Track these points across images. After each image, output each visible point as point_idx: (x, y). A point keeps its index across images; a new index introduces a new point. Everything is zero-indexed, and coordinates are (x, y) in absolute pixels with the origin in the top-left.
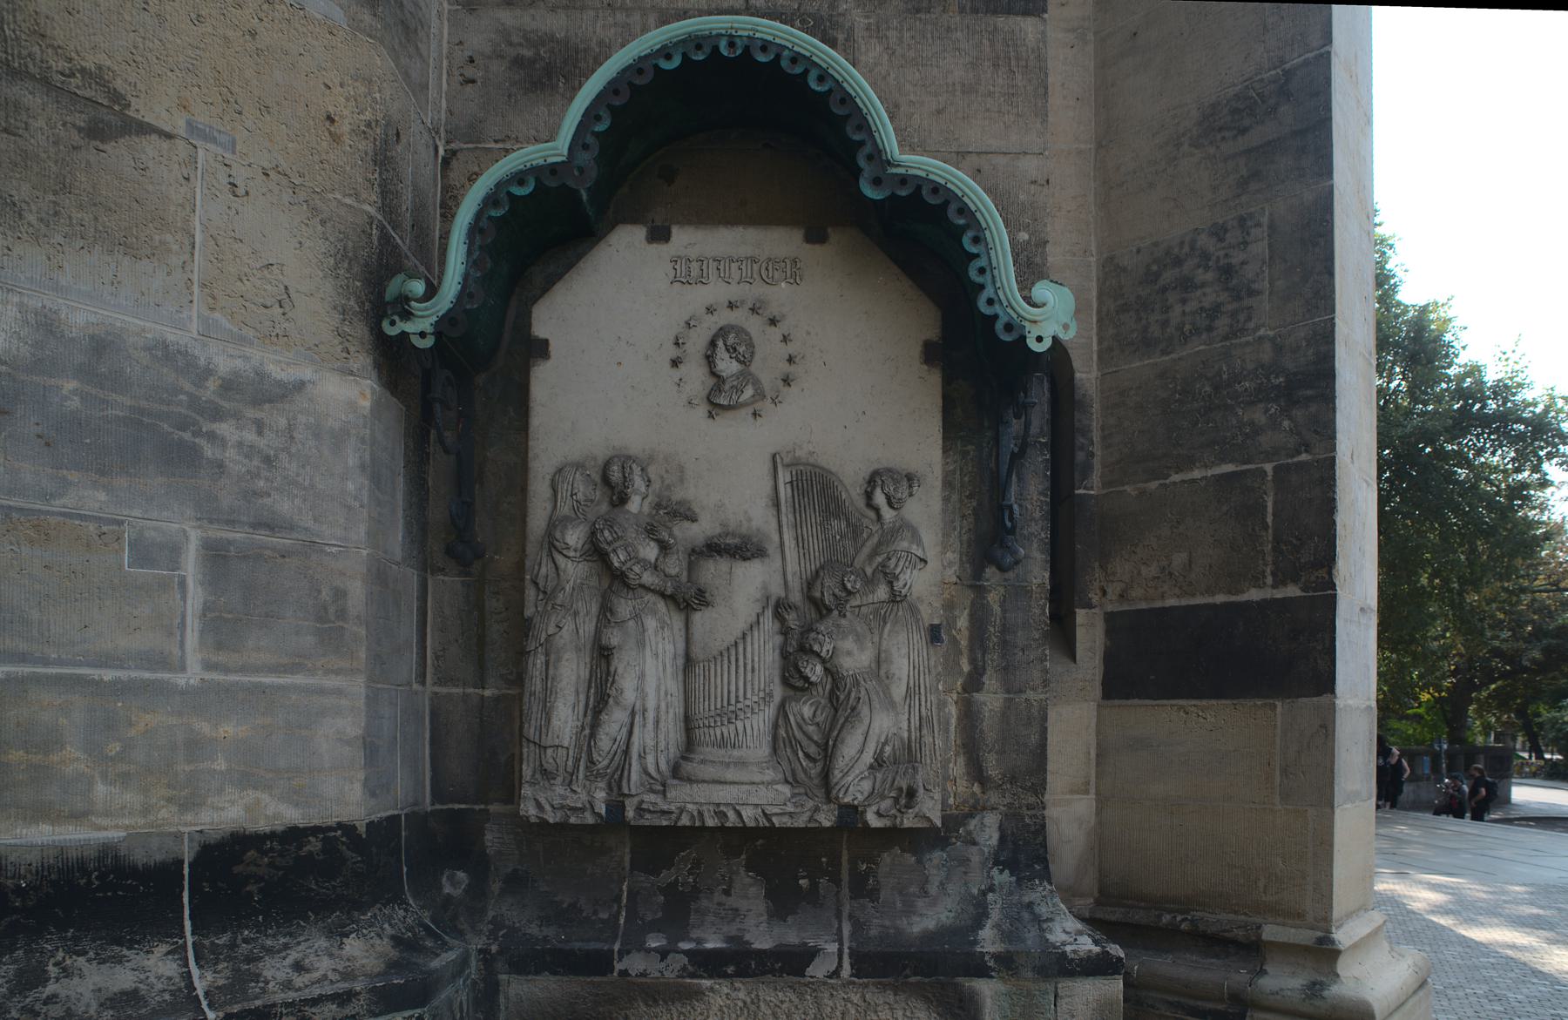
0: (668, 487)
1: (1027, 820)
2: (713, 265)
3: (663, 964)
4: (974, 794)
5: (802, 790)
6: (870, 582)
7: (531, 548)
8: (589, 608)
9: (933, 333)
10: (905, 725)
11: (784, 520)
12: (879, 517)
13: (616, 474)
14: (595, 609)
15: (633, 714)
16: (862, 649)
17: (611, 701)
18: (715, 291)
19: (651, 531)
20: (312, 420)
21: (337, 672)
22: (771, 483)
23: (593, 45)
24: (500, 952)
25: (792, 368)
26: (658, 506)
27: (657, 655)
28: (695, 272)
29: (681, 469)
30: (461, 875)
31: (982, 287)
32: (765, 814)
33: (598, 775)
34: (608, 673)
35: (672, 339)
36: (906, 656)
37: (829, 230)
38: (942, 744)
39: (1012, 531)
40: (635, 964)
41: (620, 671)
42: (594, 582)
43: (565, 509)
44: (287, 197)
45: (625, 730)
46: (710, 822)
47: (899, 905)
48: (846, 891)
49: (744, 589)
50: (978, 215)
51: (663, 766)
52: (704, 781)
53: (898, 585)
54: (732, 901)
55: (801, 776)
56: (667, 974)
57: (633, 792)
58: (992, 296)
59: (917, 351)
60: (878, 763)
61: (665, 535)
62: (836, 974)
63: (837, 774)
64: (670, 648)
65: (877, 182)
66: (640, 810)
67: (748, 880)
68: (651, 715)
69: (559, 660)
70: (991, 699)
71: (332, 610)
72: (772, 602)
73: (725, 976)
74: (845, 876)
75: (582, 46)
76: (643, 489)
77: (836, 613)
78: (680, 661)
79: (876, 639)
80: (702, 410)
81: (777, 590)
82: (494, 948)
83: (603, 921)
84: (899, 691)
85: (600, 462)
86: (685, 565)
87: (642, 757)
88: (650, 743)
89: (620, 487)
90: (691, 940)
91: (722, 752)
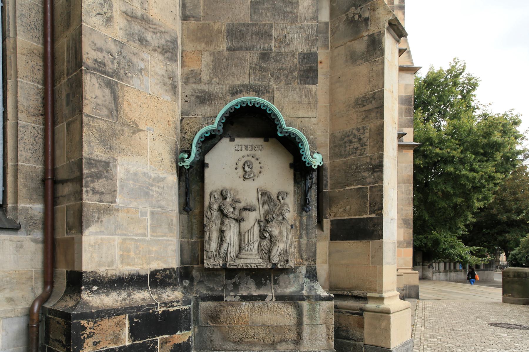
6: (278, 216)
7: (205, 209)
8: (219, 222)
13: (224, 193)
14: (220, 222)
18: (244, 153)
19: (232, 205)
21: (172, 236)
25: (261, 170)
26: (233, 200)
28: (240, 148)
29: (238, 192)
31: (303, 155)
36: (286, 231)
38: (293, 250)
39: (309, 204)
40: (228, 298)
42: (219, 216)
43: (213, 201)
46: (245, 267)
48: (272, 283)
49: (252, 218)
53: (284, 216)
54: (248, 286)
55: (264, 257)
59: (288, 166)
60: (280, 254)
61: (235, 206)
62: (271, 300)
63: (272, 257)
65: (281, 133)
66: (230, 265)
68: (232, 245)
70: (304, 241)
74: (272, 280)
78: (238, 233)
80: (242, 179)
81: (258, 218)
85: (220, 190)
88: (232, 251)
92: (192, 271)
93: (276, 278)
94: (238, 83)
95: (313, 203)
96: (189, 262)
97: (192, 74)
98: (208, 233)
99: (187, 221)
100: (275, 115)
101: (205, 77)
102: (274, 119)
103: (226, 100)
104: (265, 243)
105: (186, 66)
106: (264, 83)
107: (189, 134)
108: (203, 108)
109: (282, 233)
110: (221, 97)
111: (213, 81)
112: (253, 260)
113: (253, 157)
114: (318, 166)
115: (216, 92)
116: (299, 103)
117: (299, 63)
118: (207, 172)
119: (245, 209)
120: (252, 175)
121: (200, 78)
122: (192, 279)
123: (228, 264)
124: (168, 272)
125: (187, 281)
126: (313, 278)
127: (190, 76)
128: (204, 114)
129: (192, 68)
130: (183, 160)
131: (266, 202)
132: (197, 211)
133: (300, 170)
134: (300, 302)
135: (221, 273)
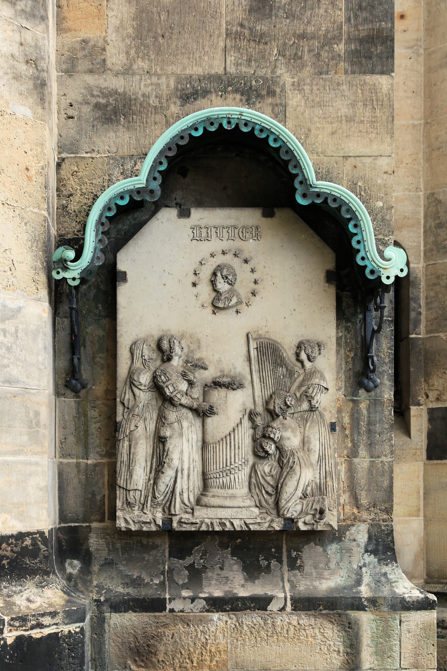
0: (192, 351)
1: (383, 528)
2: (213, 230)
3: (192, 605)
5: (264, 511)
6: (299, 400)
7: (120, 384)
9: (331, 266)
12: (303, 366)
13: (165, 345)
14: (155, 416)
15: (177, 471)
17: (166, 465)
18: (215, 245)
19: (184, 375)
20: (24, 326)
21: (36, 454)
22: (245, 349)
23: (139, 96)
24: (106, 601)
25: (256, 287)
26: (187, 362)
27: (188, 440)
28: (204, 235)
29: (199, 341)
30: (76, 562)
31: (358, 251)
34: (164, 450)
35: (193, 271)
38: (337, 486)
39: (373, 371)
40: (177, 605)
42: (154, 402)
44: (11, 214)
45: (172, 480)
46: (217, 528)
50: (357, 213)
51: (192, 499)
52: (214, 507)
53: (314, 402)
55: (264, 503)
57: (177, 513)
58: (364, 256)
59: (322, 276)
60: (305, 496)
61: (191, 377)
62: (283, 609)
64: (195, 436)
65: (304, 196)
66: (180, 522)
67: (232, 562)
68: (186, 472)
69: (136, 444)
70: (363, 461)
71: (34, 422)
72: (248, 411)
73: (225, 611)
75: (133, 97)
76: (180, 353)
77: (281, 417)
78: (200, 444)
79: (302, 430)
80: (210, 309)
82: (102, 599)
83: (156, 584)
85: (156, 338)
86: (201, 392)
87: (181, 494)
88: (185, 487)
89: (168, 352)
90: (205, 593)
91: (223, 491)
93: (294, 554)
94: (197, 71)
95: (385, 368)
97: (84, 49)
98: (126, 444)
99: (74, 412)
100: (289, 151)
101: (115, 57)
102: (286, 163)
103: (168, 113)
104: (267, 468)
105: (69, 30)
106: (261, 72)
107: (77, 198)
108: (112, 134)
109: (309, 442)
110: (155, 108)
111: (135, 67)
113: (235, 255)
114: (397, 277)
115: (144, 95)
116: (349, 120)
117: (349, 20)
118: (124, 293)
119: (217, 384)
120: (234, 300)
121: (104, 60)
124: (28, 542)
126: (384, 553)
127: (80, 55)
129: (83, 35)
130: (63, 264)
131: (268, 366)
132: (99, 389)
134: (353, 614)
135: (158, 541)
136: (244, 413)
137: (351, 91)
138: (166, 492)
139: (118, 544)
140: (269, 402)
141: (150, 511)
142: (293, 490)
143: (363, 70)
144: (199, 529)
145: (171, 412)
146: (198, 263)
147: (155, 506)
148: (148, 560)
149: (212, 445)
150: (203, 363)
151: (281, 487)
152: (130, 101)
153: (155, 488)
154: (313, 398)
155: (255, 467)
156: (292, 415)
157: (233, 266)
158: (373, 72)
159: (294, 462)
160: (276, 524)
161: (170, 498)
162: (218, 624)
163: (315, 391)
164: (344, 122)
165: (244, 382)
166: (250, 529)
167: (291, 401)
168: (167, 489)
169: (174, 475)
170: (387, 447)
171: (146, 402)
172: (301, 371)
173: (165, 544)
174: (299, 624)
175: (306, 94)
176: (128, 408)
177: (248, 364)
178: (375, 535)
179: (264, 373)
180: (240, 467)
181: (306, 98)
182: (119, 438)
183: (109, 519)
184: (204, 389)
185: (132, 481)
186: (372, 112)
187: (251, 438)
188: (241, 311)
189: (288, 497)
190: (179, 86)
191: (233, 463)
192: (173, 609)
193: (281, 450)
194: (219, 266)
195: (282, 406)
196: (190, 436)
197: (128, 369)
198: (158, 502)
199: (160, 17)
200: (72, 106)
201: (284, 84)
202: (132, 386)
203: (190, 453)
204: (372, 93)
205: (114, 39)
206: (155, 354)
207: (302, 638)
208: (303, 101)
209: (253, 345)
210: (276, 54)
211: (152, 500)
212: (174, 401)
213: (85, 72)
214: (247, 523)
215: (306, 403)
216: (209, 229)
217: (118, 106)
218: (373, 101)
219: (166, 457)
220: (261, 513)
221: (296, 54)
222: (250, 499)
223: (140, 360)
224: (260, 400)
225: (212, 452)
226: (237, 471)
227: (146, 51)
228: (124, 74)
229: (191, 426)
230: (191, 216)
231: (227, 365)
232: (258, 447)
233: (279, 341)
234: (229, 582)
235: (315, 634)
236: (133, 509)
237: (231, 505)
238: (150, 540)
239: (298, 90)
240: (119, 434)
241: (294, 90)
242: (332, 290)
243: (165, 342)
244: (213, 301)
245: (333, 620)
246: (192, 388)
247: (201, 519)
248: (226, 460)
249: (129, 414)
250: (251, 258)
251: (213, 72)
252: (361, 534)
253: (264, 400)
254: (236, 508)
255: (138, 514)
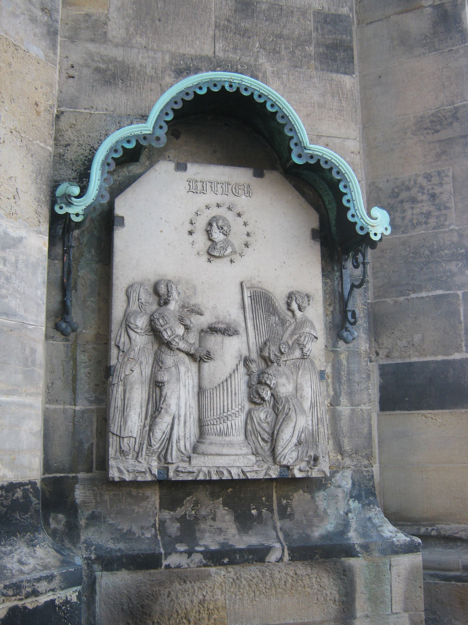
2: (209, 185)
3: (189, 560)
4: (338, 460)
7: (115, 327)
9: (316, 225)
10: (310, 423)
11: (247, 315)
12: (294, 315)
13: (162, 289)
16: (289, 383)
17: (163, 411)
18: (210, 198)
19: (181, 320)
22: (239, 297)
23: (137, 66)
26: (183, 307)
27: (185, 386)
28: (200, 187)
29: (194, 288)
32: (243, 472)
33: (154, 452)
34: (161, 395)
35: (189, 221)
37: (265, 171)
40: (173, 560)
41: (169, 395)
42: (150, 346)
43: (134, 307)
45: (169, 427)
46: (215, 477)
47: (305, 522)
48: (276, 516)
51: (188, 447)
52: (211, 455)
53: (305, 350)
54: (218, 524)
55: (260, 451)
56: (191, 565)
57: (174, 461)
59: (308, 233)
60: (299, 443)
61: (188, 322)
62: (280, 560)
63: (279, 449)
64: (191, 382)
66: (177, 471)
67: (224, 512)
68: (182, 419)
69: (132, 389)
73: (223, 564)
75: (131, 66)
76: (177, 298)
77: (275, 364)
78: (196, 390)
79: (295, 378)
80: (206, 257)
82: (93, 557)
83: (148, 539)
84: (307, 405)
87: (178, 441)
88: (182, 434)
89: (166, 297)
90: (200, 546)
91: (220, 438)
92: (73, 490)
94: (190, 51)
96: (67, 466)
97: (87, 21)
98: (121, 388)
101: (115, 30)
103: (163, 83)
104: (263, 414)
106: (246, 59)
107: (74, 148)
108: (110, 95)
110: (152, 77)
111: (134, 41)
112: (234, 458)
113: (229, 208)
115: (141, 65)
116: (321, 106)
117: (317, 29)
118: (121, 238)
119: (213, 330)
121: (105, 33)
122: (72, 510)
123: (172, 468)
124: (19, 494)
125: (61, 516)
128: (112, 108)
129: (86, 10)
133: (338, 240)
135: (148, 492)
136: (240, 359)
137: (321, 84)
138: (162, 439)
139: (106, 496)
140: (264, 349)
141: (145, 459)
142: (288, 437)
143: (330, 69)
144: (196, 478)
145: (168, 356)
146: (194, 213)
147: (150, 454)
148: (138, 512)
149: (209, 391)
150: (199, 309)
151: (277, 434)
152: (128, 68)
153: (151, 435)
154: (305, 346)
155: (251, 413)
156: (285, 362)
157: (227, 218)
158: (338, 72)
159: (290, 409)
160: (272, 472)
161: (166, 445)
162: (216, 579)
163: (307, 339)
164: (316, 107)
165: (239, 329)
166: (247, 477)
167: (285, 348)
168: (164, 436)
169: (171, 421)
170: (365, 396)
171: (142, 346)
172: (292, 321)
173: (156, 495)
174: (296, 574)
175: (284, 82)
176: (123, 352)
177: (243, 312)
178: (358, 481)
179: (258, 321)
180: (237, 413)
181: (284, 85)
182: (113, 383)
183: (97, 469)
184: (200, 334)
185: (127, 428)
186: (339, 102)
187: (246, 384)
188: (235, 261)
189: (285, 444)
190: (174, 62)
191: (230, 410)
192: (169, 565)
193: (276, 397)
194: (214, 217)
195: (277, 353)
196: (187, 381)
197: (124, 312)
198: (154, 450)
199: (157, 5)
200: (73, 67)
201: (265, 72)
202: (128, 328)
203: (186, 399)
204: (338, 88)
205: (115, 17)
206: (151, 298)
207: (299, 588)
208: (282, 87)
209: (247, 294)
210: (258, 47)
211: (147, 448)
212: (172, 345)
213: (87, 41)
214: (245, 471)
215: (298, 350)
216: (205, 183)
217: (117, 72)
218: (339, 94)
219: (163, 402)
220: (257, 461)
221: (274, 49)
222: (247, 447)
223: (137, 303)
224: (255, 347)
225: (209, 398)
226: (234, 418)
227: (144, 30)
228: (123, 46)
229: (188, 371)
230: (187, 170)
231: (222, 312)
232: (254, 393)
233: (271, 291)
234: (222, 534)
235: (312, 583)
236: (127, 457)
237: (228, 453)
238: (141, 491)
239: (278, 77)
240: (113, 378)
241: (274, 77)
242: (317, 247)
243: (163, 286)
244: (209, 249)
245: (329, 569)
246: (188, 333)
247: (198, 468)
248: (224, 406)
249: (124, 358)
250: (244, 212)
251: (204, 54)
252: (345, 480)
253: (258, 347)
254: (233, 455)
255: (133, 463)
